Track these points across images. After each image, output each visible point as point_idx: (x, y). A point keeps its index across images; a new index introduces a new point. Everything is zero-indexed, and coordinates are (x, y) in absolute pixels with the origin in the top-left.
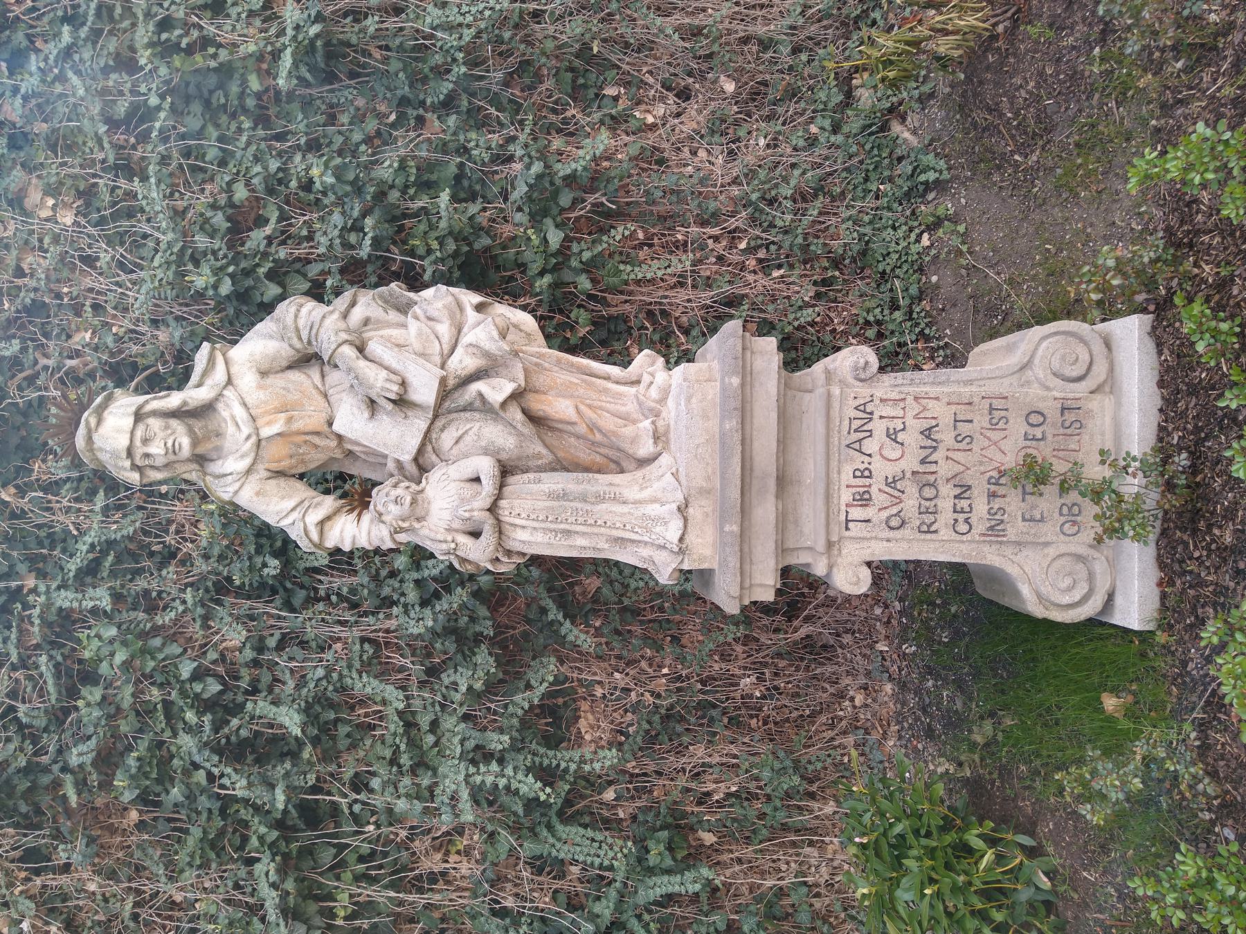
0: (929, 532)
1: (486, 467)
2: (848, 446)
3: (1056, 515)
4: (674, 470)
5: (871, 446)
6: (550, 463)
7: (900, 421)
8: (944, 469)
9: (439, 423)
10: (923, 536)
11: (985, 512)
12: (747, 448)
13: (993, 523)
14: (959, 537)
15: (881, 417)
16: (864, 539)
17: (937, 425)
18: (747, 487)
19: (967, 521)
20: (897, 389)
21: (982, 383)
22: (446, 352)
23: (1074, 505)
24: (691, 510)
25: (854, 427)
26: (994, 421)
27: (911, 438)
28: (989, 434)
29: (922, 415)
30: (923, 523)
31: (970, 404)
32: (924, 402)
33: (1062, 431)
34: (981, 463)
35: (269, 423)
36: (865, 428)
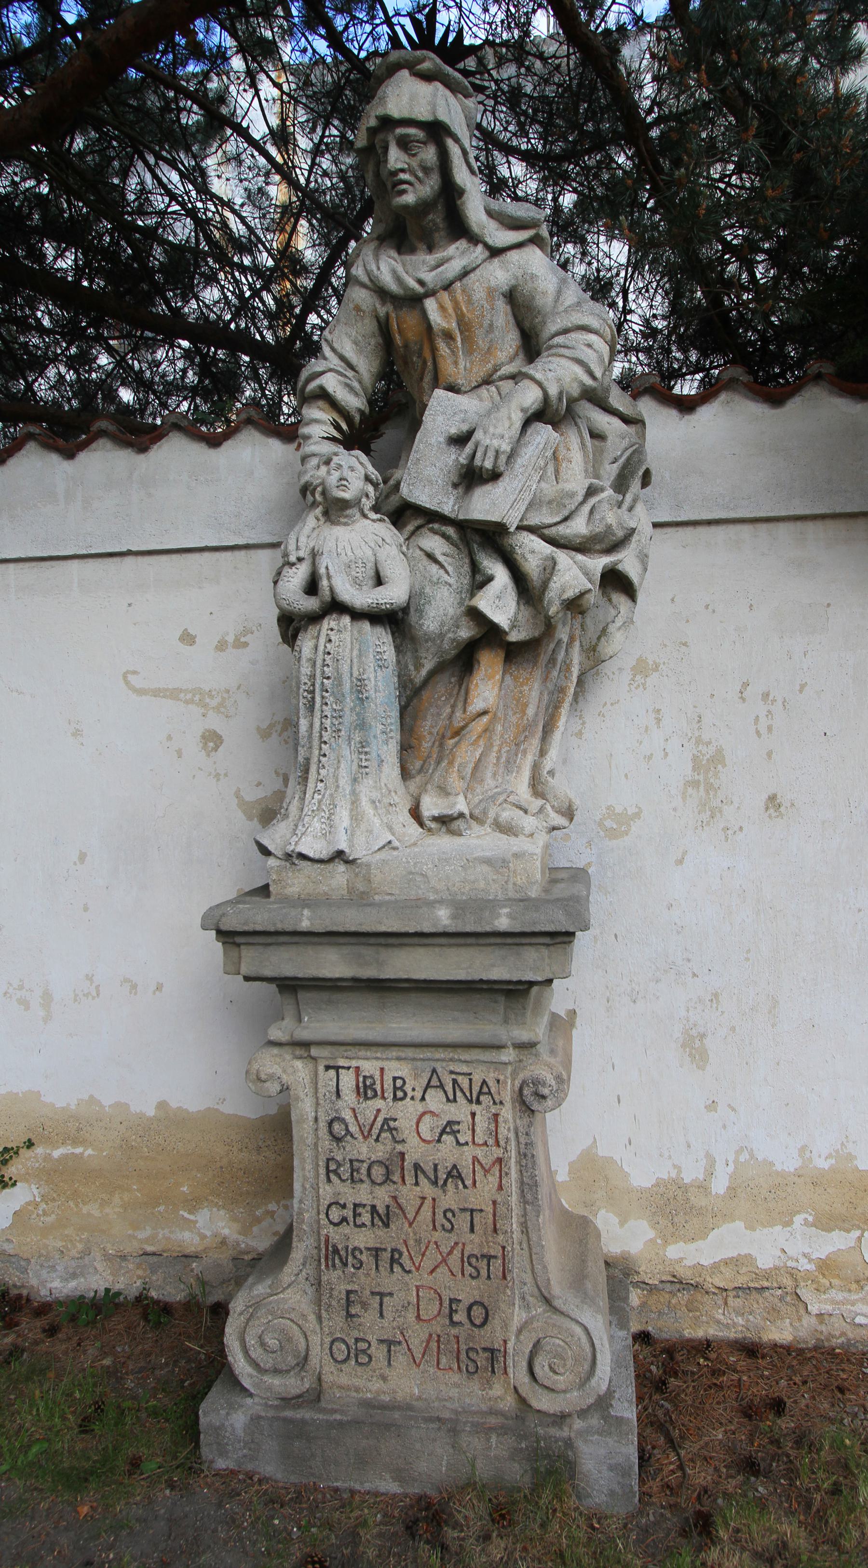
1: (393, 594)
2: (434, 1071)
3: (356, 1334)
4: (396, 843)
5: (435, 1099)
6: (411, 681)
8: (409, 1194)
9: (450, 531)
11: (356, 1244)
12: (416, 940)
13: (343, 1253)
14: (323, 1209)
15: (473, 1115)
17: (465, 1187)
18: (363, 940)
19: (344, 1220)
20: (512, 1135)
21: (525, 1246)
22: (546, 532)
24: (341, 868)
25: (460, 1079)
26: (473, 1261)
27: (447, 1153)
28: (457, 1253)
29: (478, 1167)
30: (339, 1165)
31: (495, 1230)
32: (497, 1167)
33: (464, 1347)
34: (418, 1241)
35: (442, 308)
36: (459, 1094)
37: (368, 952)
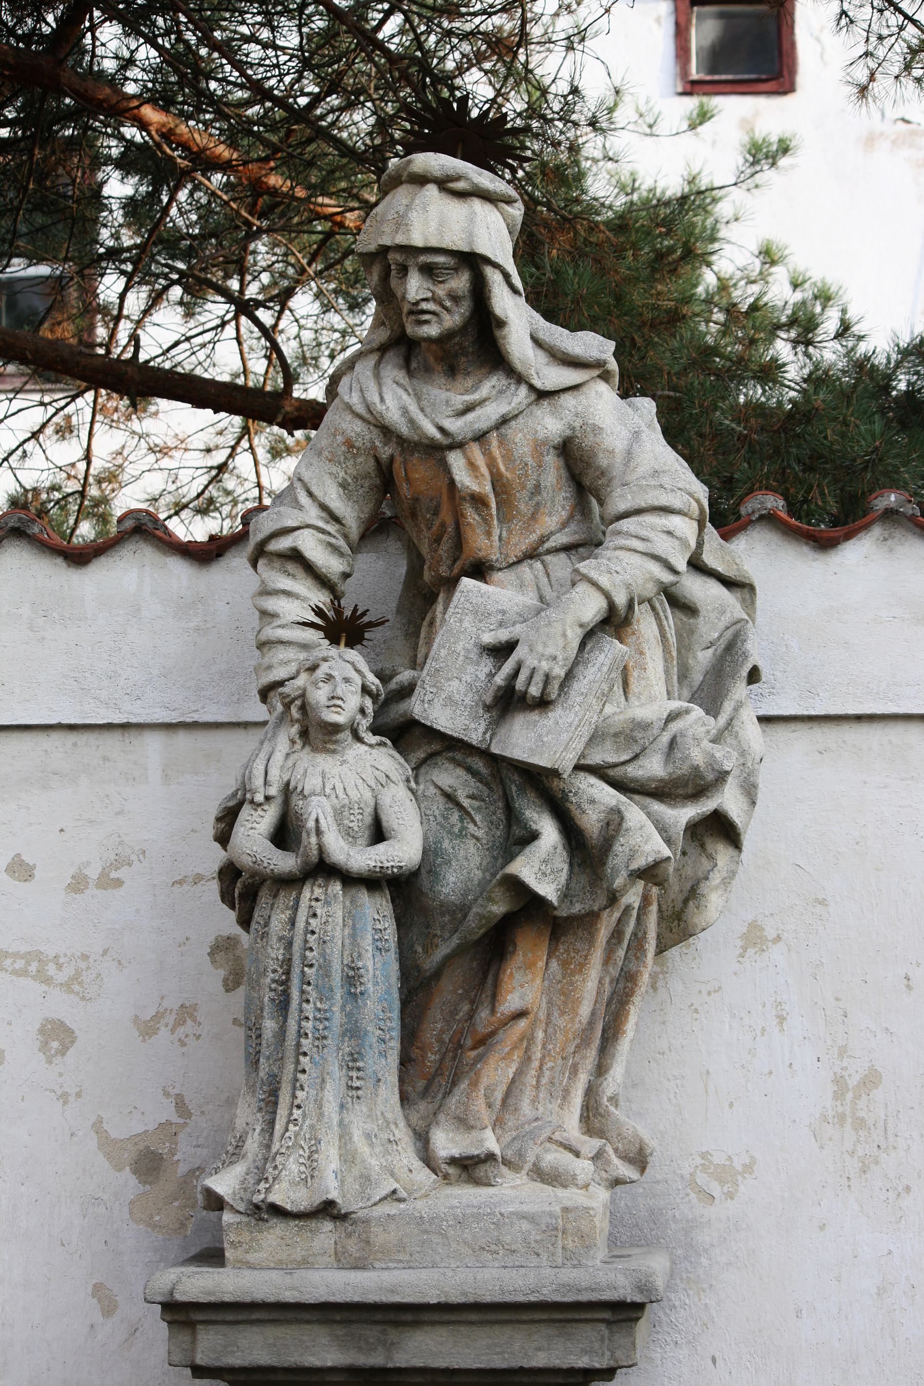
1: (403, 851)
4: (403, 1194)
6: (418, 968)
9: (479, 764)
12: (436, 1317)
22: (611, 772)
24: (328, 1226)
35: (472, 466)
37: (372, 1333)
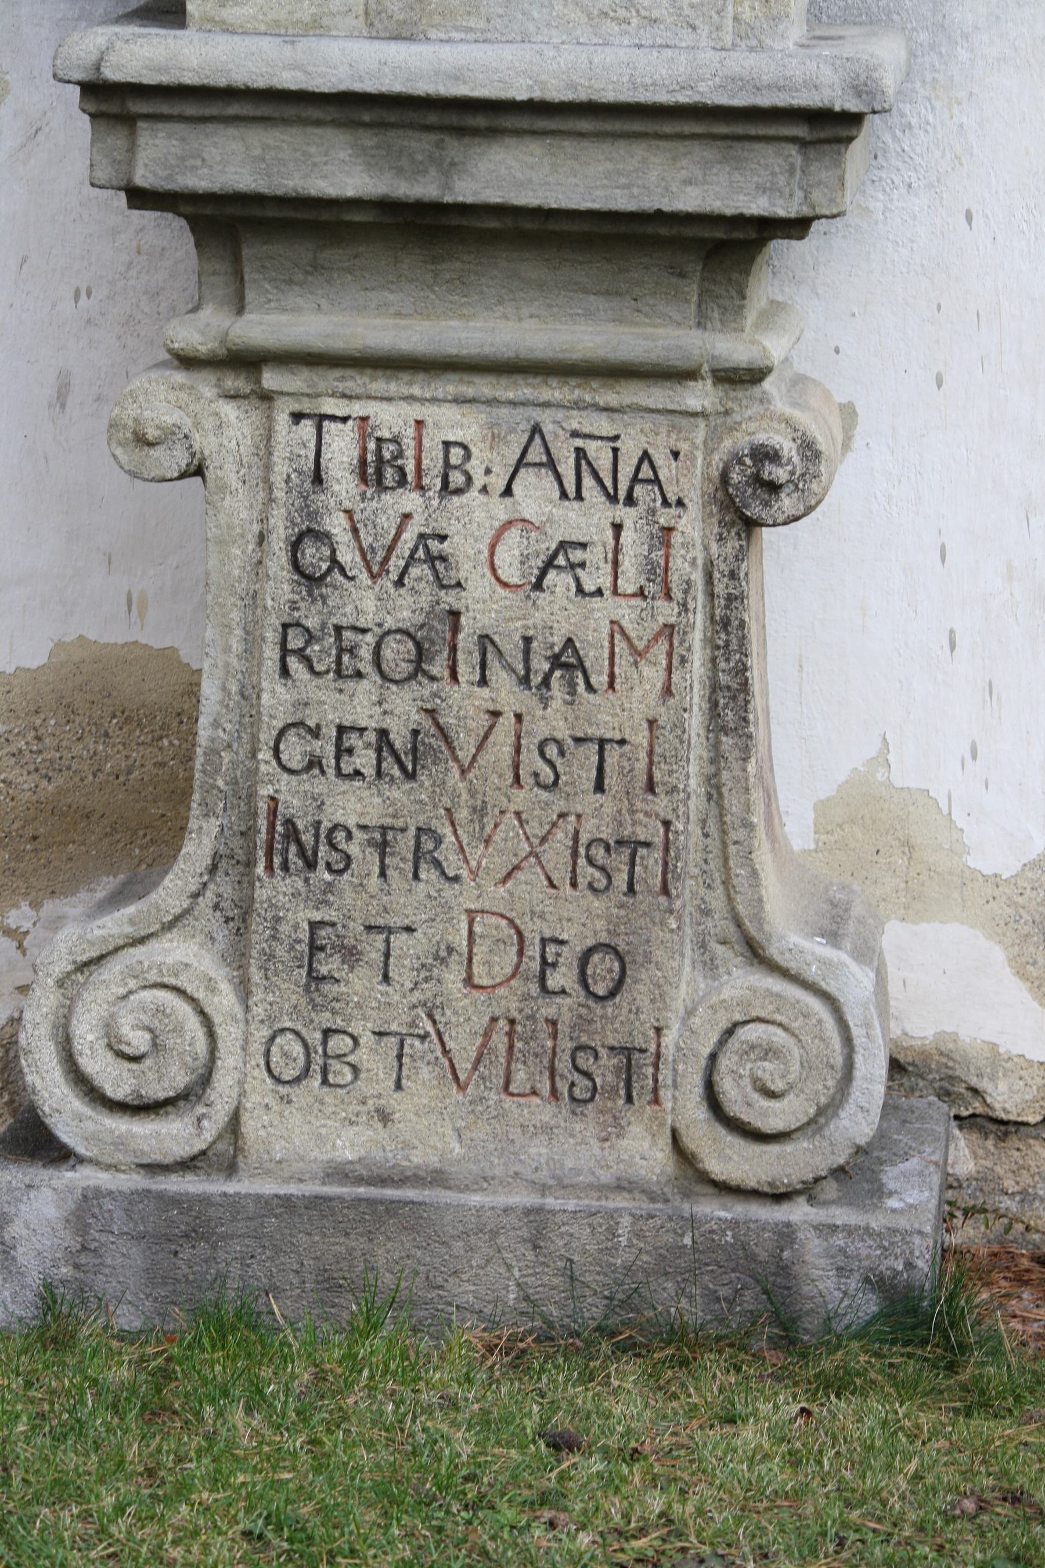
0: (285, 652)
2: (536, 430)
3: (325, 1019)
5: (535, 494)
7: (606, 582)
8: (464, 703)
10: (272, 636)
11: (339, 817)
12: (524, 122)
13: (307, 838)
14: (266, 737)
15: (617, 528)
16: (268, 467)
17: (590, 688)
18: (411, 116)
19: (314, 763)
20: (698, 577)
21: (713, 828)
23: (355, 1069)
25: (591, 447)
26: (598, 853)
27: (558, 612)
28: (561, 838)
29: (620, 646)
30: (311, 638)
31: (651, 787)
32: (660, 651)
33: (566, 1045)
34: (479, 812)
36: (588, 481)
37: (421, 144)
